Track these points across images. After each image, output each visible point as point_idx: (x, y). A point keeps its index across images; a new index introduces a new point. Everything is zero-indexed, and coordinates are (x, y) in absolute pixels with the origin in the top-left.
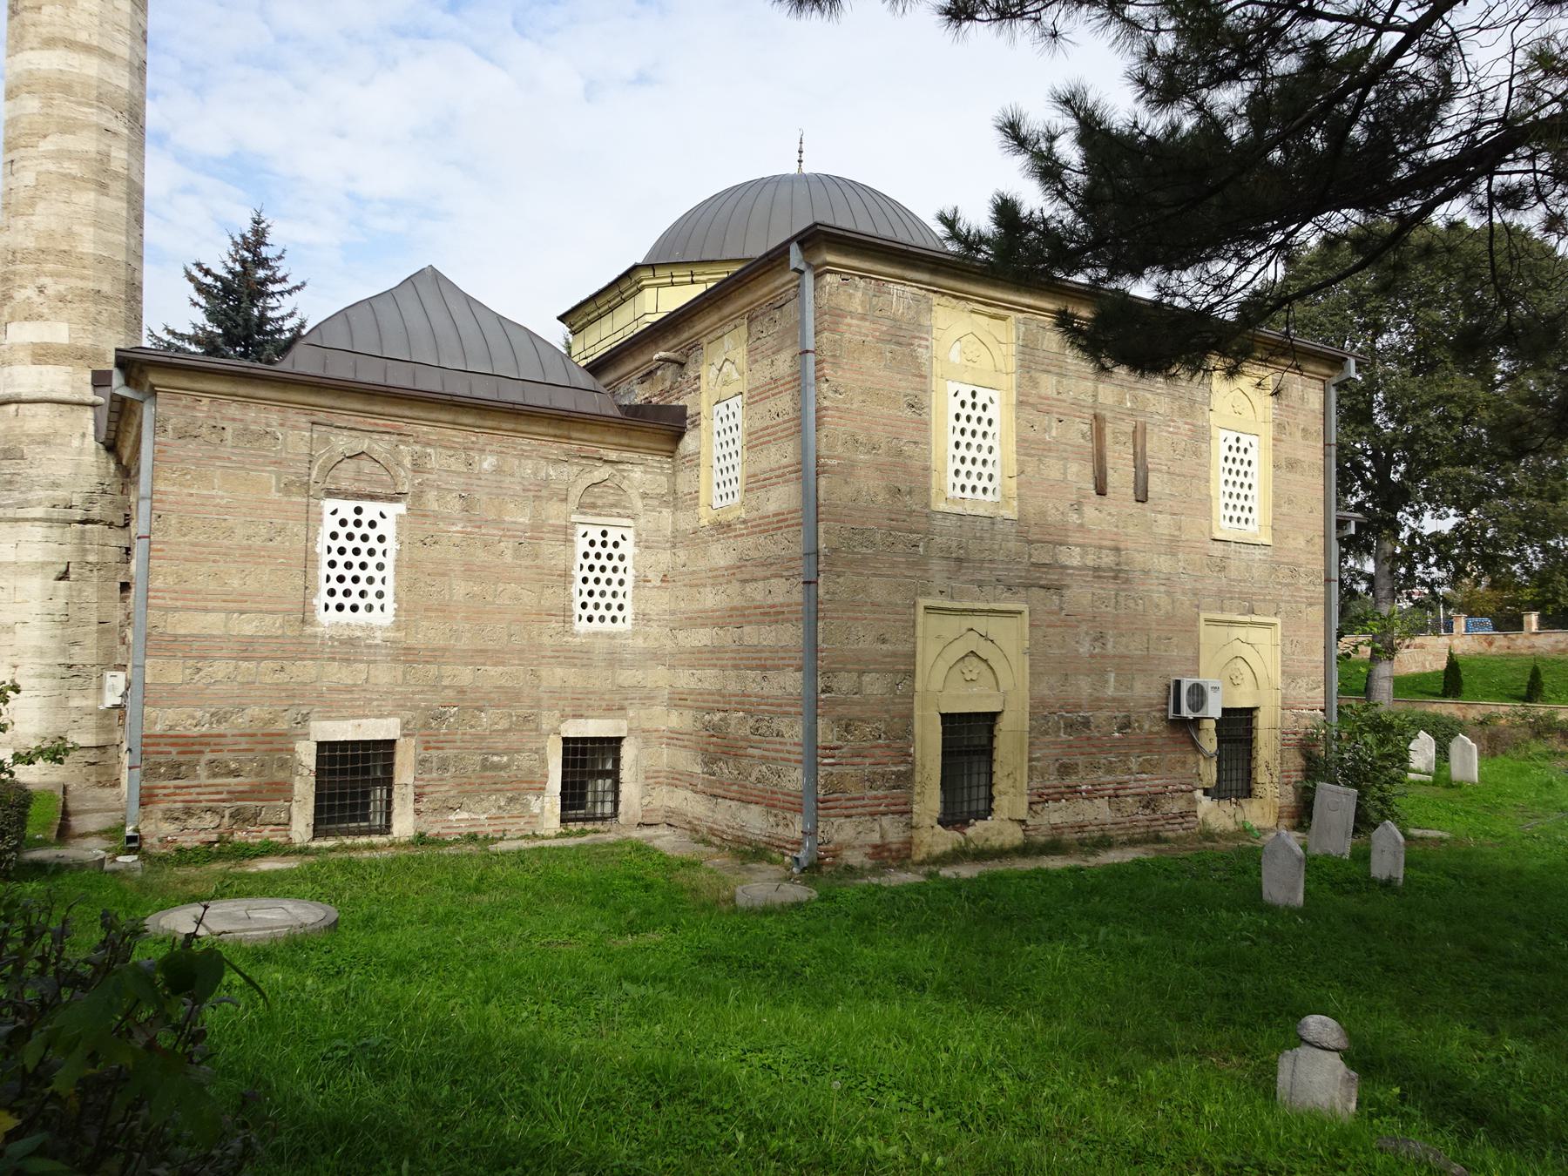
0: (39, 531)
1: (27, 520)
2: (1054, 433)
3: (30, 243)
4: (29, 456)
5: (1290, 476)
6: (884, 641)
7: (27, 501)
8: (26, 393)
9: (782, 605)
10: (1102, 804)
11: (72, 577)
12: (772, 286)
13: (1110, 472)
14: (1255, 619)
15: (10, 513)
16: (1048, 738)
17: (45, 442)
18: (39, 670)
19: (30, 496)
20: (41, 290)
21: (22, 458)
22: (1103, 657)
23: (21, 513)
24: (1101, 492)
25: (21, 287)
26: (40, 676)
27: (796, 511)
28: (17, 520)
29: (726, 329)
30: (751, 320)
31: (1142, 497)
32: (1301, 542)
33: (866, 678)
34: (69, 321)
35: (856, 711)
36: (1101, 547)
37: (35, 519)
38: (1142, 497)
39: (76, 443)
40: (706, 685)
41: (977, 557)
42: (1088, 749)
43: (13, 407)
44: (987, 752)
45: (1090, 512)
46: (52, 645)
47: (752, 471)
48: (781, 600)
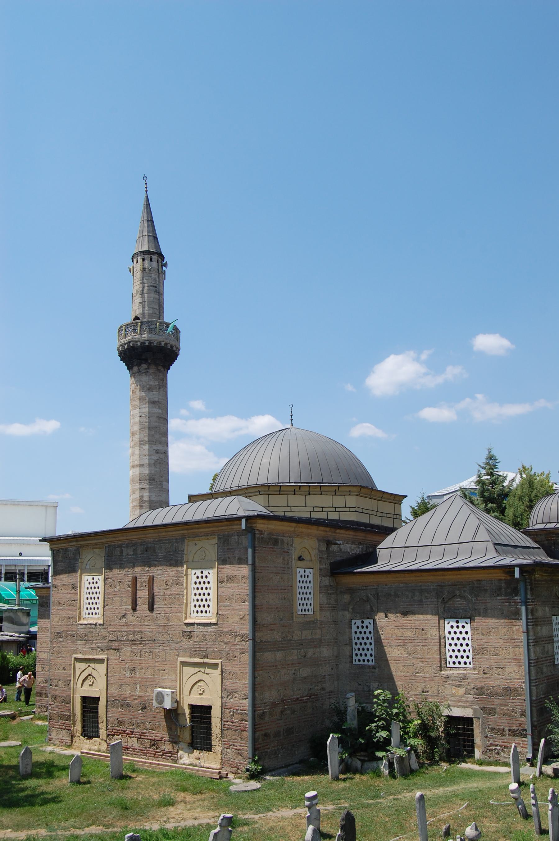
2: (118, 588)
5: (229, 585)
6: (65, 670)
10: (134, 740)
13: (138, 599)
14: (207, 660)
16: (114, 709)
22: (135, 678)
24: (134, 609)
31: (151, 608)
32: (237, 619)
33: (60, 682)
35: (57, 693)
36: (134, 632)
38: (151, 608)
41: (91, 639)
42: (129, 716)
44: (96, 711)
45: (130, 617)
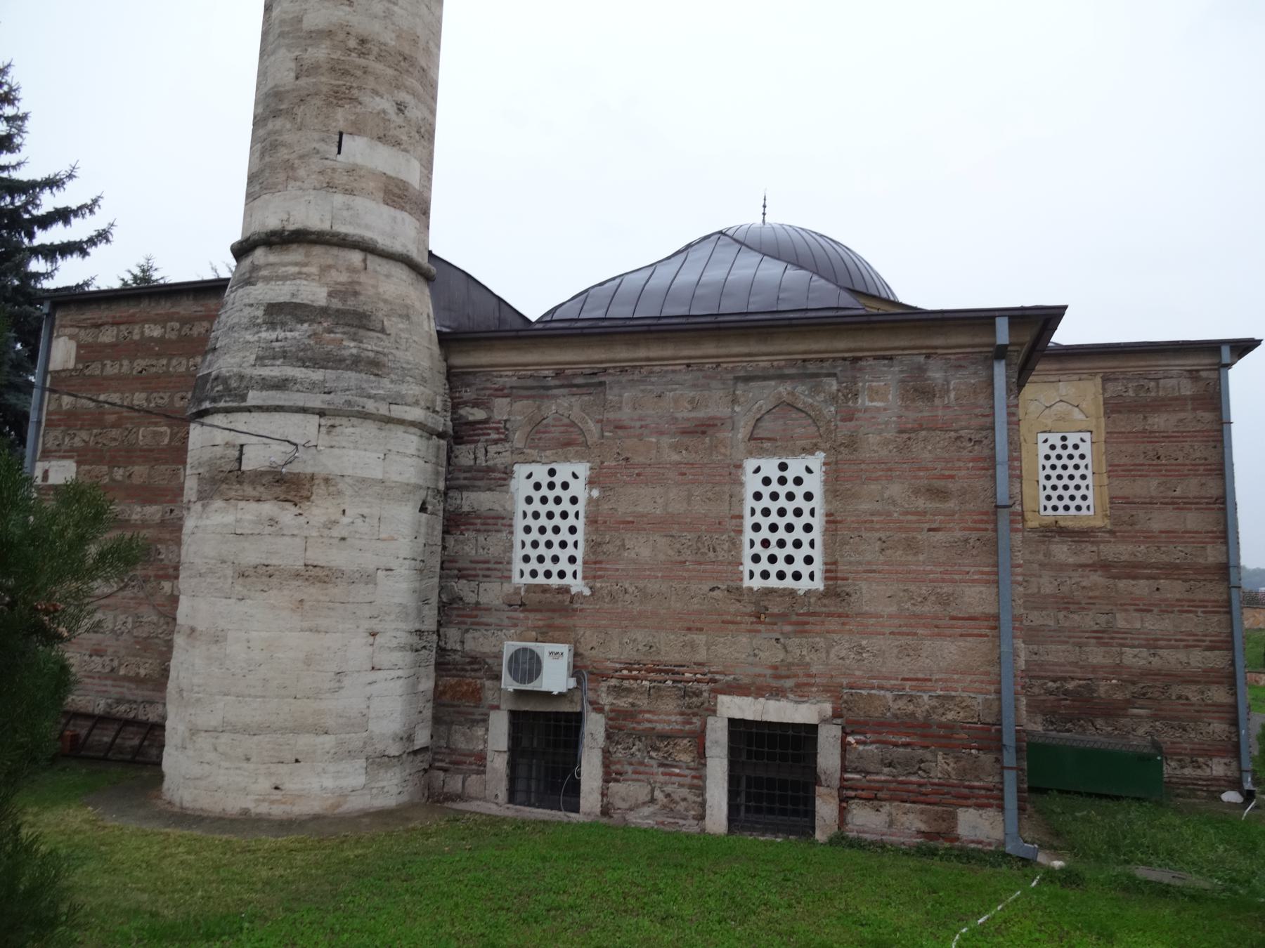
0: (411, 442)
1: (401, 422)
3: (389, 38)
4: (392, 331)
7: (399, 394)
8: (383, 242)
9: (1178, 600)
11: (430, 508)
12: (1153, 363)
15: (383, 410)
17: (408, 317)
18: (404, 638)
19: (404, 389)
20: (401, 108)
21: (383, 331)
23: (397, 411)
25: (376, 92)
26: (402, 648)
27: (1196, 532)
28: (389, 420)
29: (1062, 378)
30: (1105, 380)
34: (420, 160)
37: (413, 424)
39: (425, 323)
40: (1050, 658)
43: (356, 257)
46: (409, 600)
47: (1120, 494)
48: (1178, 596)
